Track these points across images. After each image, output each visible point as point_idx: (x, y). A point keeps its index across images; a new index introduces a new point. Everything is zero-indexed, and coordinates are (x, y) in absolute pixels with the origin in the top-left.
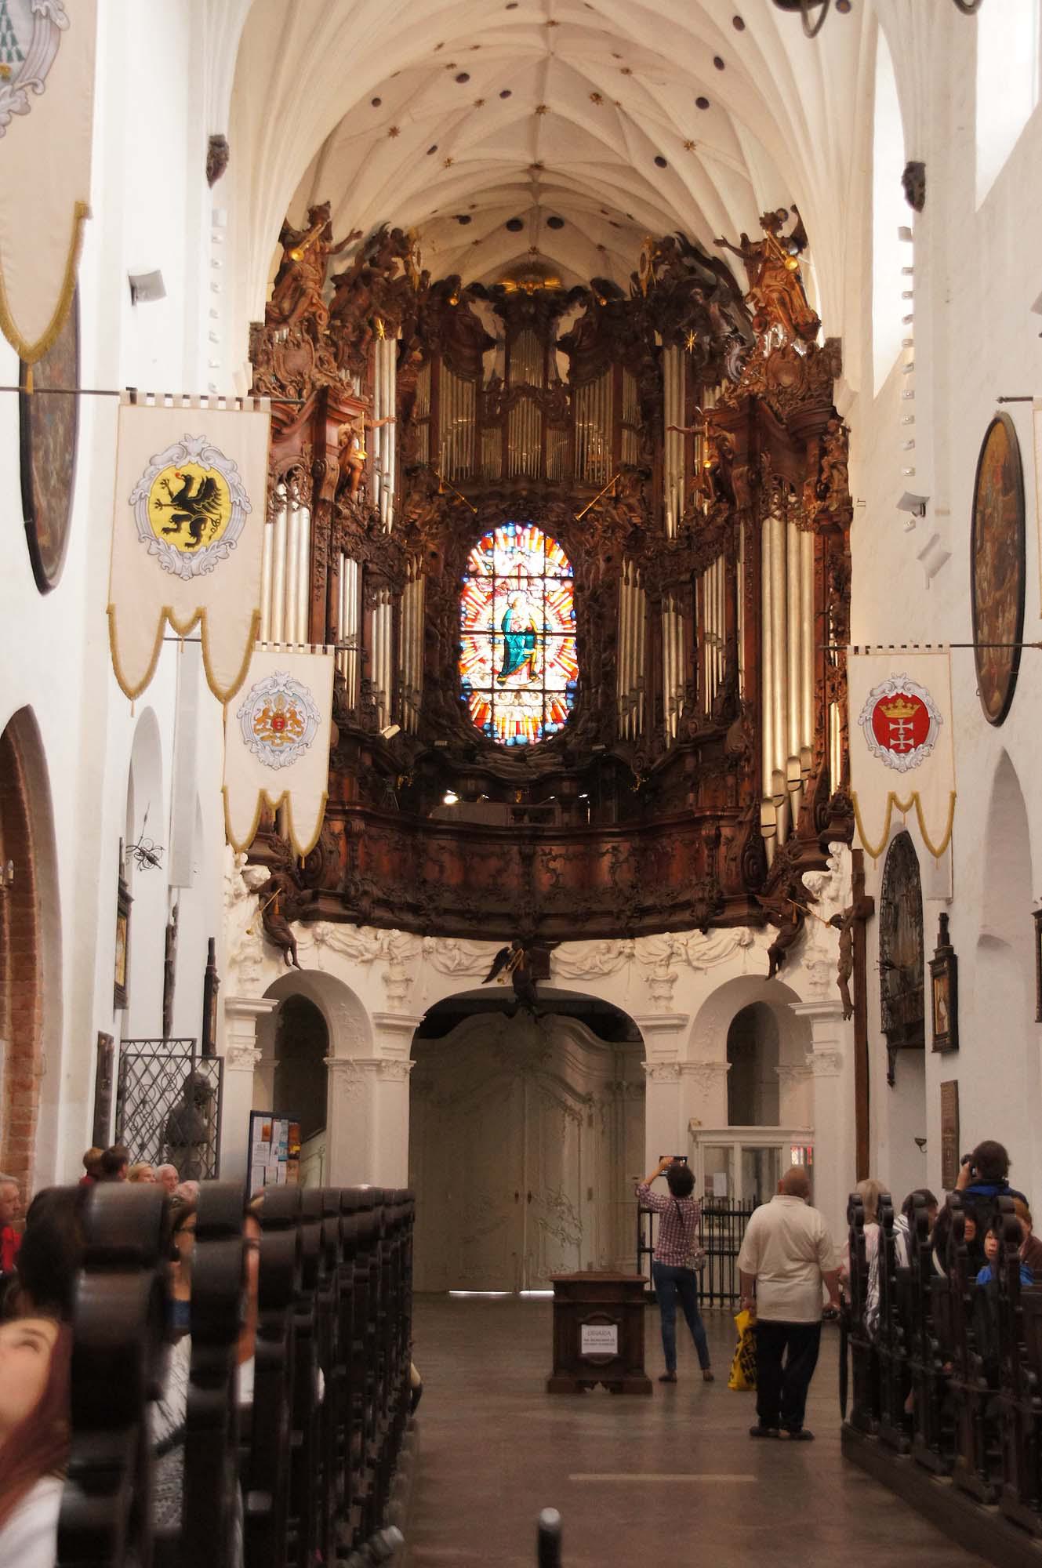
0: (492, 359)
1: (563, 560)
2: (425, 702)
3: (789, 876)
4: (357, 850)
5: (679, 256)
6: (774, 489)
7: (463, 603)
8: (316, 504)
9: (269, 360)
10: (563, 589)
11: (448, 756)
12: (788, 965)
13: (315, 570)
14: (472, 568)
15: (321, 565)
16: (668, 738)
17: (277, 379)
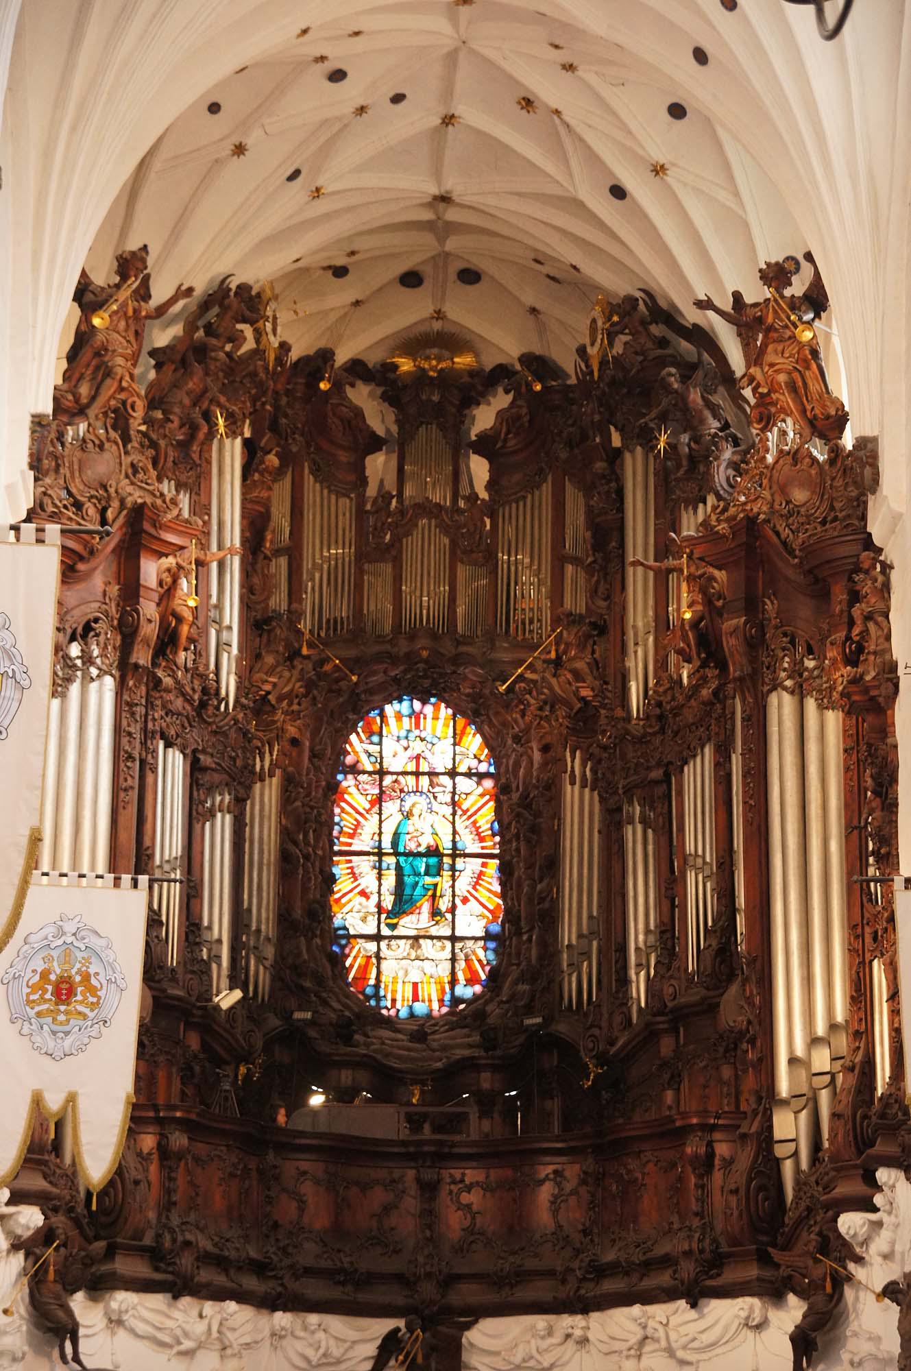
0: (379, 465)
1: (480, 749)
2: (280, 956)
3: (819, 1218)
4: (175, 1179)
5: (644, 323)
6: (784, 649)
7: (337, 810)
8: (125, 670)
9: (58, 466)
10: (480, 790)
11: (313, 1033)
12: (820, 1360)
13: (122, 765)
14: (349, 760)
15: (130, 757)
16: (635, 1009)
17: (70, 493)
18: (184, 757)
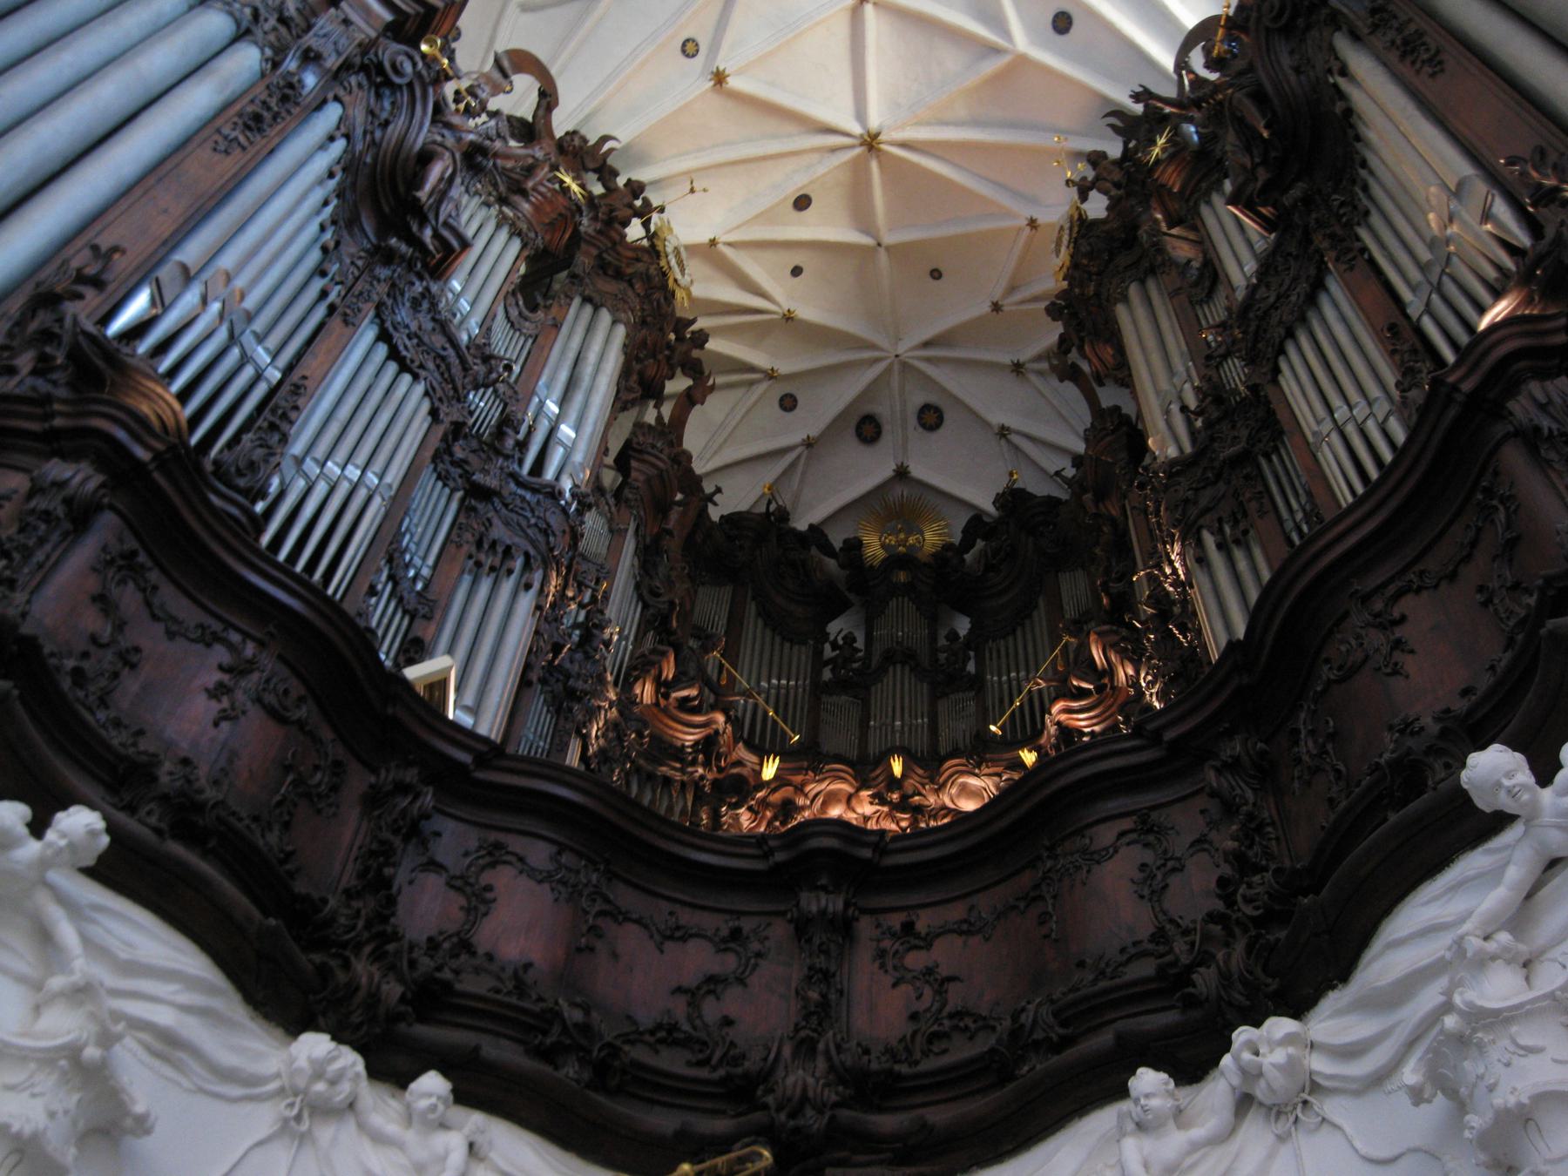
18: (434, 413)
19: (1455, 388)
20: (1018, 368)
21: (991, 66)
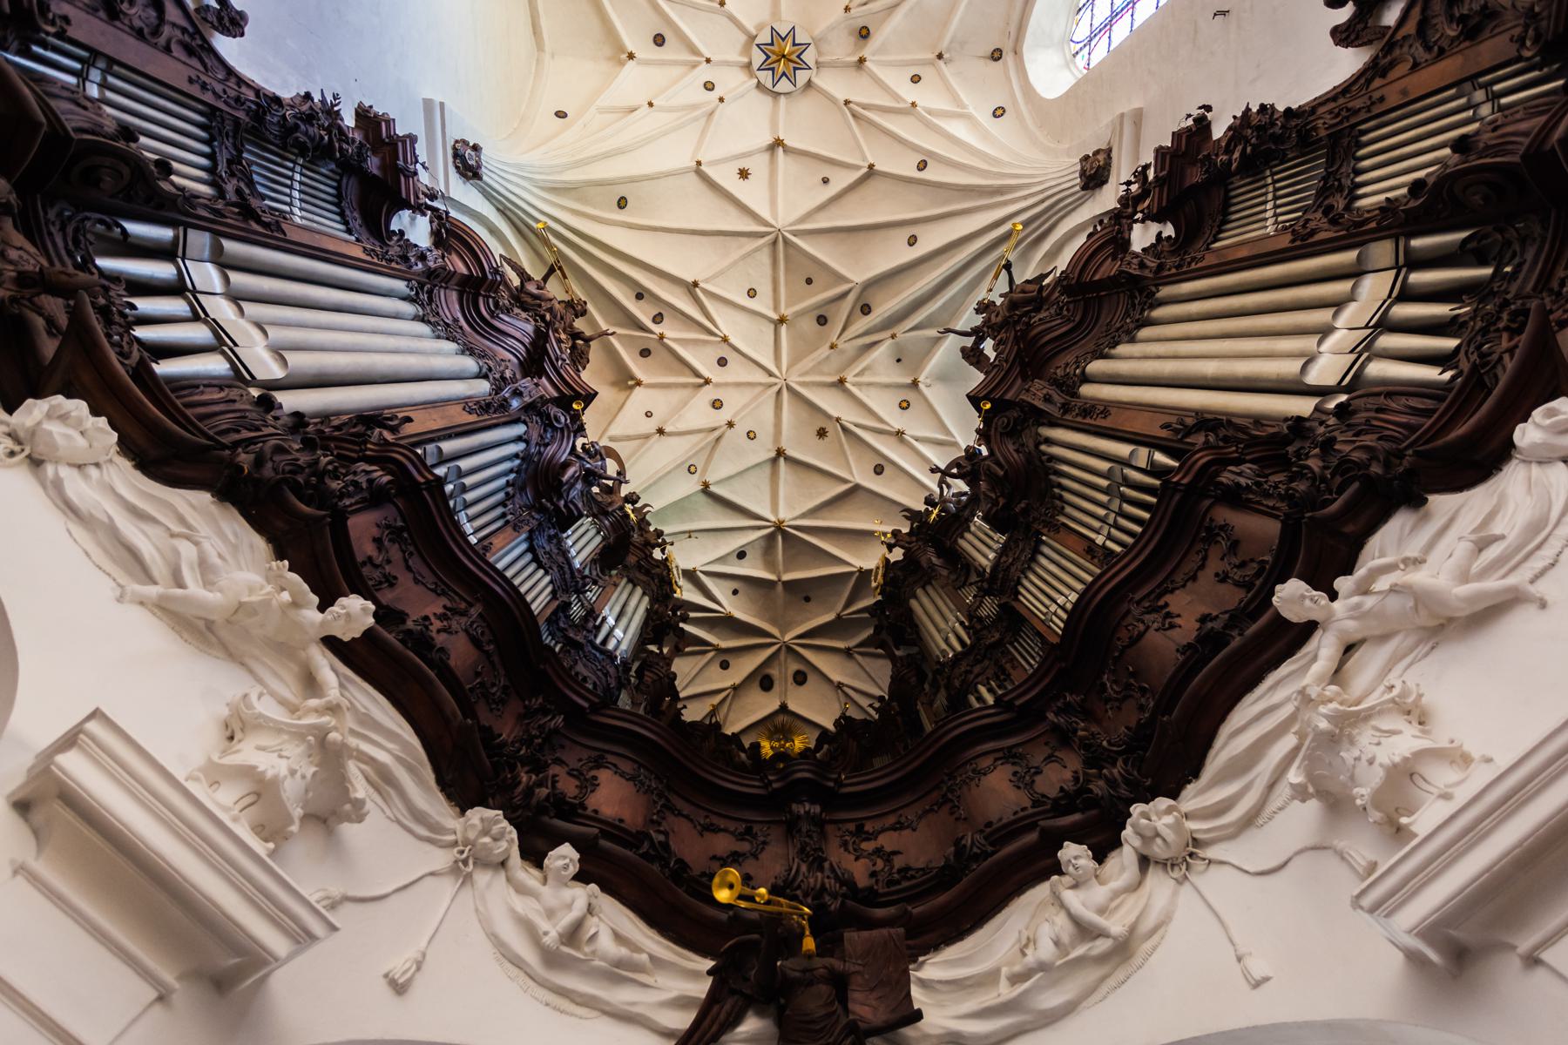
18: (554, 592)
19: (1177, 483)
20: (848, 653)
21: (843, 488)
